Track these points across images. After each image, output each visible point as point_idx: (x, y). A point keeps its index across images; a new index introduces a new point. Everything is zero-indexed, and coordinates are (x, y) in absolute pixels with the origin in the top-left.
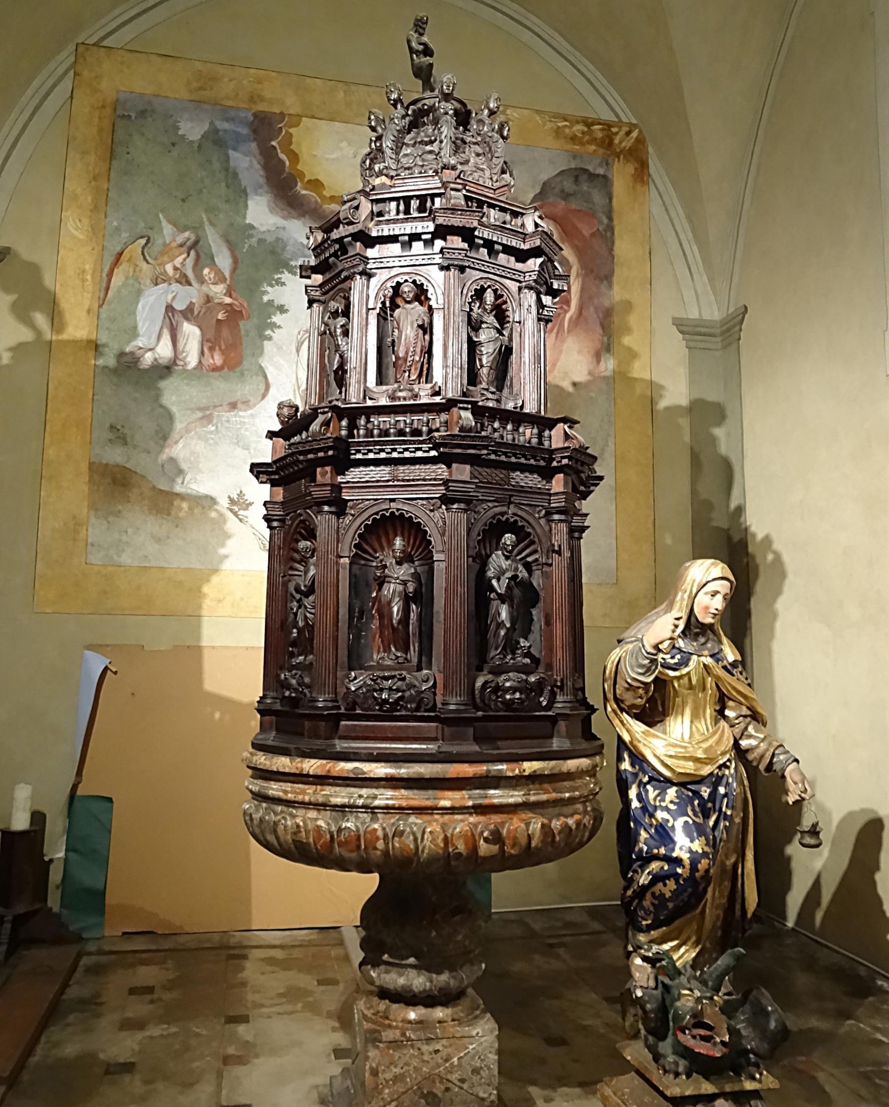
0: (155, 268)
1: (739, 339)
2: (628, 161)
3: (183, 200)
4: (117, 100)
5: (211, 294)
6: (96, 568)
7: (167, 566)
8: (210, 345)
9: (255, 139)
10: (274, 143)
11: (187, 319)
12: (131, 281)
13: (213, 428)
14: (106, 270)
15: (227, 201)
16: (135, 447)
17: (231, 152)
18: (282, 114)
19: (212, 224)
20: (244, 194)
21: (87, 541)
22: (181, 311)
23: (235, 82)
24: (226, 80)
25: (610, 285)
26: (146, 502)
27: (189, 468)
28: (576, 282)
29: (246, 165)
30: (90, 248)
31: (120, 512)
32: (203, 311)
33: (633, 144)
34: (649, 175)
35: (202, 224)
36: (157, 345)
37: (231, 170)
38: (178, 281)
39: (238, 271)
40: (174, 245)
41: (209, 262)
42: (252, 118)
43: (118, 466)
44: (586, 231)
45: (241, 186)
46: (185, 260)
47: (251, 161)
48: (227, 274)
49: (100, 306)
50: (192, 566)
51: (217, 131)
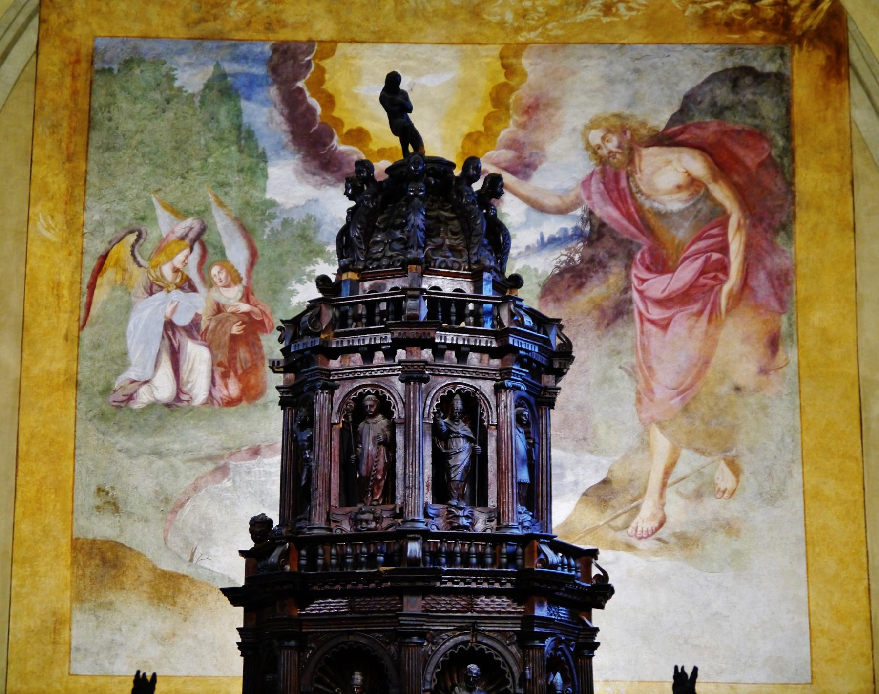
0: (149, 272)
2: (815, 47)
4: (95, 49)
5: (222, 301)
7: (173, 674)
8: (223, 369)
9: (275, 81)
10: (301, 84)
11: (193, 337)
14: (87, 279)
15: (241, 171)
16: (130, 515)
17: (244, 104)
18: (311, 42)
19: (221, 204)
20: (263, 157)
21: (70, 644)
25: (790, 236)
26: (145, 588)
27: (200, 540)
28: (738, 238)
29: (264, 119)
30: (66, 253)
31: (111, 603)
32: (213, 324)
33: (823, 21)
34: (849, 64)
36: (154, 376)
37: (243, 129)
38: (180, 287)
39: (256, 268)
40: (173, 237)
41: (218, 257)
42: (270, 53)
44: (750, 159)
45: (257, 147)
46: (187, 257)
47: (271, 112)
48: (242, 271)
50: (204, 673)
51: (224, 76)
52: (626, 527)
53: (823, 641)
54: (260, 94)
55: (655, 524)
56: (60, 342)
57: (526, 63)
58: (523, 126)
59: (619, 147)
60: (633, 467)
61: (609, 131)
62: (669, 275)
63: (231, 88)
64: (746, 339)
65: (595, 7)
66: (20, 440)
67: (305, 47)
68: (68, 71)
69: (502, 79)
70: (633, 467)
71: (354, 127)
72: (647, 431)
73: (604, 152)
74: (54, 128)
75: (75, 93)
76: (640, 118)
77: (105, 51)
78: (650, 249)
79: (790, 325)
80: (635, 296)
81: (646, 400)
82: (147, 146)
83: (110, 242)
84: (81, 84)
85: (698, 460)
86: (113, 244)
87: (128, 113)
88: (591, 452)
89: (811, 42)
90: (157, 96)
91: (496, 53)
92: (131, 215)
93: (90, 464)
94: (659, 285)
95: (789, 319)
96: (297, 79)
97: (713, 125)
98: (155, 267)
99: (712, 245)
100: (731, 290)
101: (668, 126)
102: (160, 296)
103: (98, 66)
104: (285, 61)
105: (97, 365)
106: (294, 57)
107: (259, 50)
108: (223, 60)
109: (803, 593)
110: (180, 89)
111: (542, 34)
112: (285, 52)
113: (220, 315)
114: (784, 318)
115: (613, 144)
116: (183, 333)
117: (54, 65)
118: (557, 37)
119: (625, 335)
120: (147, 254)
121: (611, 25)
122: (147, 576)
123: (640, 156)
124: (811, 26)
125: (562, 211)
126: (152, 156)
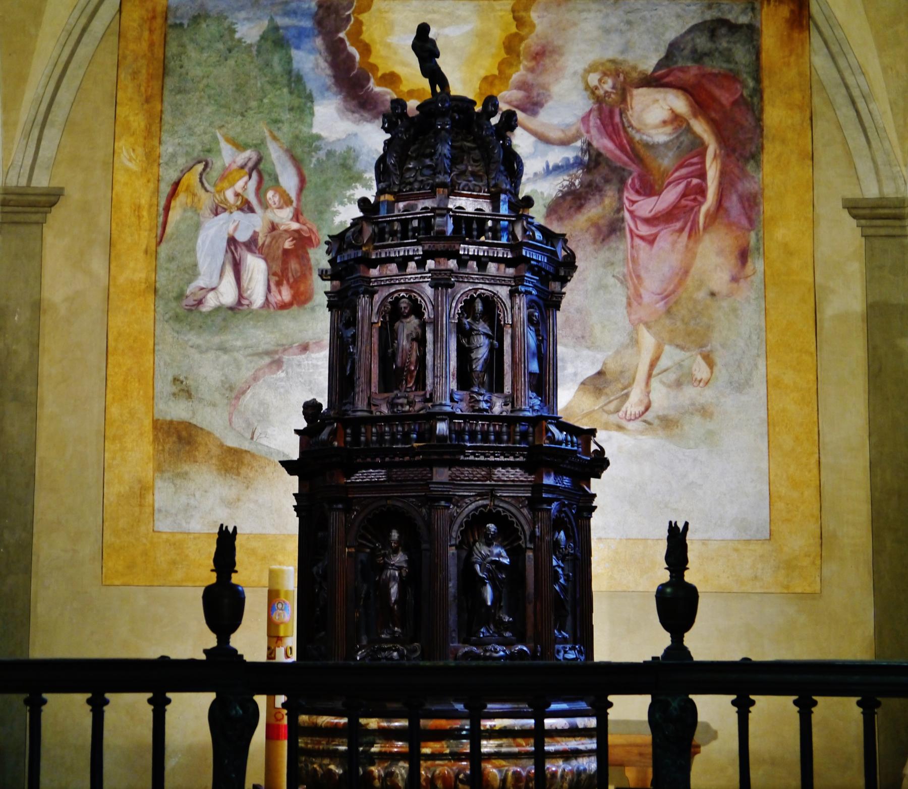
0: (214, 196)
3: (243, 115)
4: (168, 8)
5: (276, 220)
6: (164, 536)
8: (277, 278)
9: (320, 33)
10: (342, 35)
11: (250, 250)
12: (189, 214)
14: (163, 203)
15: (291, 109)
16: (201, 400)
17: (294, 53)
19: (275, 138)
20: (310, 98)
22: (245, 244)
27: (259, 421)
29: (311, 65)
30: (145, 181)
31: (186, 473)
32: (268, 240)
34: (810, 17)
35: (263, 142)
36: (219, 284)
37: (294, 73)
38: (240, 209)
39: (305, 192)
40: (234, 167)
41: (272, 183)
42: (316, 9)
44: (725, 98)
45: (305, 89)
46: (246, 183)
47: (316, 59)
48: (293, 195)
50: (264, 532)
51: (276, 28)
52: (617, 411)
53: (780, 505)
54: (307, 44)
55: (642, 409)
56: (141, 255)
58: (532, 70)
59: (614, 87)
61: (605, 74)
62: (656, 198)
64: (720, 252)
66: (110, 338)
68: (146, 26)
69: (514, 29)
70: (624, 361)
71: (387, 72)
72: (635, 330)
73: (601, 92)
74: (135, 75)
75: (152, 45)
76: (632, 63)
77: (177, 8)
78: (639, 175)
79: (758, 240)
80: (627, 215)
81: (635, 304)
82: (213, 89)
83: (182, 171)
84: (157, 37)
86: (183, 173)
87: (197, 61)
88: (588, 348)
90: (220, 46)
91: (509, 7)
92: (200, 147)
93: (167, 358)
94: (647, 206)
95: (757, 235)
96: (338, 31)
98: (219, 192)
99: (692, 172)
100: (708, 210)
101: (655, 70)
102: (223, 216)
103: (171, 21)
104: (329, 15)
105: (172, 275)
106: (337, 12)
107: (306, 6)
108: (276, 15)
109: (765, 465)
110: (240, 40)
112: (328, 8)
113: (274, 233)
114: (753, 234)
115: (608, 85)
116: (243, 247)
119: (618, 248)
120: (213, 180)
122: (215, 451)
123: (631, 96)
126: (217, 98)
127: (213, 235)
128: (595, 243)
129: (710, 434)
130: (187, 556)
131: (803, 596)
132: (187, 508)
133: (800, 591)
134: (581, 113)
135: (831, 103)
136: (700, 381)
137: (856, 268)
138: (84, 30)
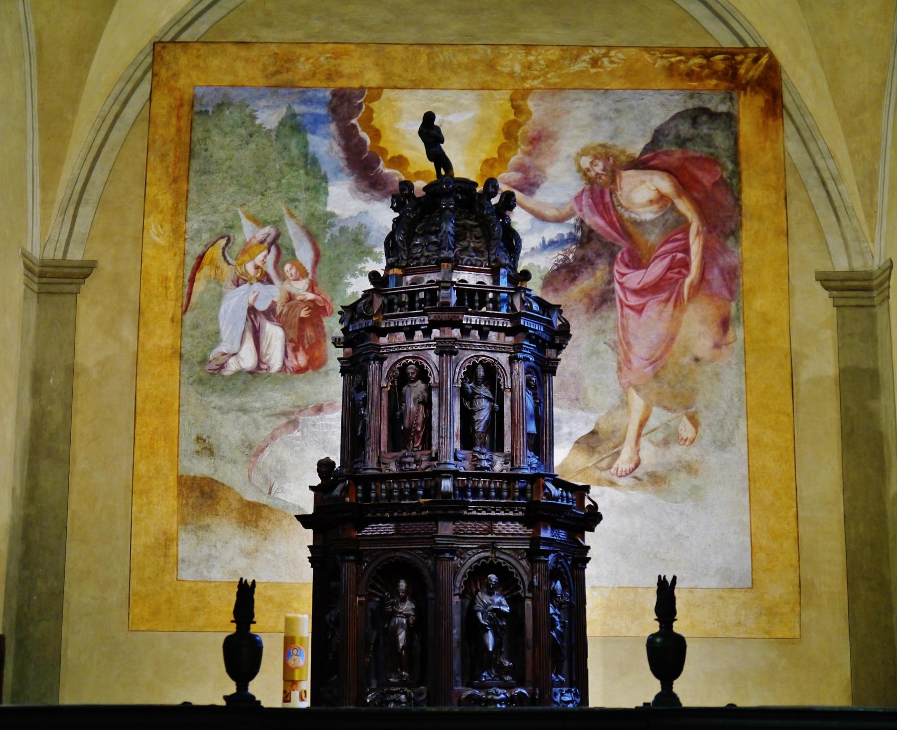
0: (236, 269)
1: (888, 297)
2: (756, 93)
3: (263, 195)
4: (194, 96)
5: (293, 291)
6: (187, 584)
8: (293, 345)
9: (334, 119)
10: (354, 121)
12: (213, 285)
13: (299, 434)
14: (188, 275)
15: (307, 189)
16: (222, 457)
17: (310, 137)
18: (362, 89)
19: (292, 216)
20: (325, 179)
22: (263, 312)
23: (311, 61)
24: (303, 59)
25: (738, 240)
29: (326, 149)
31: (208, 526)
32: (286, 309)
33: (762, 72)
34: (783, 106)
35: (281, 219)
36: (240, 350)
37: (309, 157)
38: (260, 280)
39: (319, 265)
40: (255, 242)
43: (204, 478)
44: (707, 180)
45: (320, 171)
46: (265, 257)
47: (331, 144)
49: (184, 312)
50: (281, 580)
51: (294, 115)
52: (609, 467)
53: (761, 556)
54: (323, 129)
55: (632, 466)
56: (168, 323)
57: (531, 104)
58: (528, 154)
59: (604, 170)
60: (615, 421)
62: (644, 271)
63: (300, 124)
64: (703, 321)
65: (585, 61)
67: (357, 92)
68: (174, 113)
70: (615, 421)
71: (396, 155)
73: (592, 174)
74: (163, 157)
75: (179, 130)
77: (203, 97)
78: (628, 250)
79: (738, 310)
80: (617, 287)
81: (625, 369)
82: (235, 170)
84: (184, 123)
85: (665, 416)
86: (208, 247)
87: (220, 145)
88: (582, 409)
89: (753, 89)
90: (242, 131)
91: (508, 97)
92: (223, 224)
94: (635, 278)
95: (737, 305)
96: (351, 118)
97: (678, 153)
98: (240, 265)
99: (677, 247)
100: (692, 283)
101: (642, 154)
102: (244, 287)
103: (196, 109)
104: (342, 103)
105: (196, 341)
106: (350, 101)
107: (322, 95)
108: (294, 103)
109: (746, 518)
110: (260, 126)
111: (543, 82)
112: (342, 97)
114: (733, 304)
115: (599, 168)
116: (262, 316)
117: (163, 108)
118: (555, 84)
119: (609, 317)
120: (234, 254)
121: (597, 74)
122: (235, 505)
123: (621, 177)
124: (753, 76)
125: (559, 220)
127: (234, 304)
128: (587, 312)
129: (696, 489)
130: (209, 603)
131: (782, 640)
132: (209, 558)
133: (780, 636)
134: (574, 193)
135: (803, 185)
136: (686, 440)
137: (829, 336)
138: (117, 117)
